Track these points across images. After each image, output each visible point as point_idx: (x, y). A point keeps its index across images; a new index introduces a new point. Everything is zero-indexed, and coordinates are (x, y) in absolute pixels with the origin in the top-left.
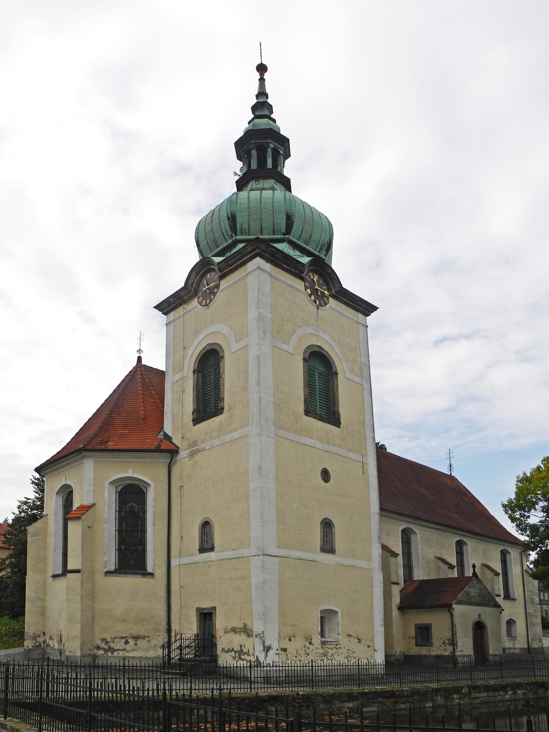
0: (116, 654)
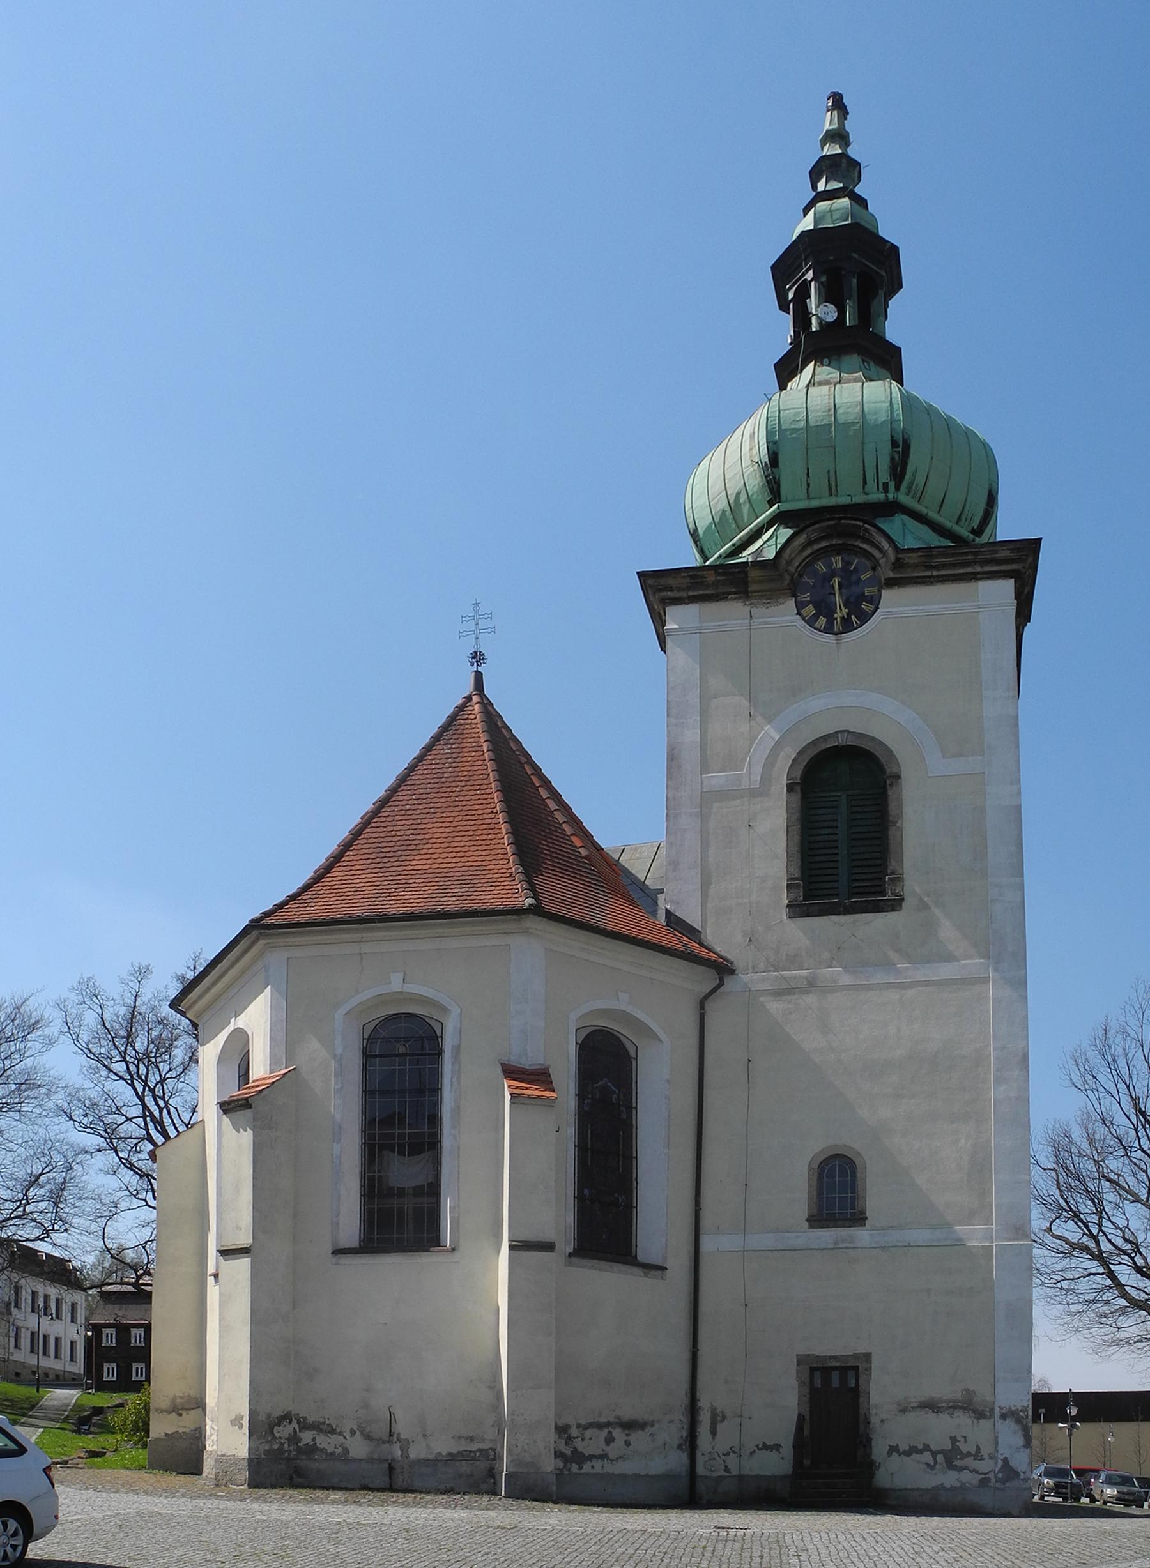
0: (587, 1467)
